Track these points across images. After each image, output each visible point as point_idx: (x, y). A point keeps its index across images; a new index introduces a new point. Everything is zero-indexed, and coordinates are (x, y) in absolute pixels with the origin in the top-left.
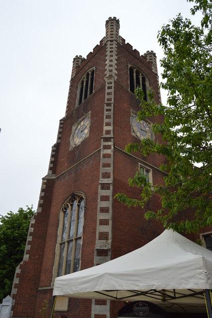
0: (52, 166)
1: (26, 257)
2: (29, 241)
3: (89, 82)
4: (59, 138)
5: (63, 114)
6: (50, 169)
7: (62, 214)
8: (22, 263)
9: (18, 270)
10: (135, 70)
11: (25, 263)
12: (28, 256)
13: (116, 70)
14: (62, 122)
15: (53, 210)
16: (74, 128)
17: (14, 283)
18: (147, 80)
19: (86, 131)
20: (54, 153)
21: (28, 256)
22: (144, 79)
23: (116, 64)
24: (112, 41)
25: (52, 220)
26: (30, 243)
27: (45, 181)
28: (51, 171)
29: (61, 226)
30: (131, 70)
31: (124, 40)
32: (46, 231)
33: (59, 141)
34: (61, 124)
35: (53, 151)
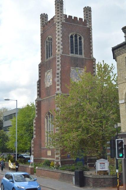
0: (38, 86)
1: (34, 136)
2: (34, 130)
3: (50, 46)
4: (40, 77)
5: (39, 61)
6: (38, 95)
7: (46, 119)
8: (33, 139)
9: (32, 141)
10: (74, 35)
11: (35, 138)
12: (35, 136)
13: (62, 45)
14: (40, 66)
15: (42, 116)
16: (46, 74)
17: (32, 146)
18: (82, 37)
19: (51, 80)
20: (38, 86)
21: (35, 136)
22: (80, 38)
23: (62, 41)
24: (58, 23)
25: (42, 121)
26: (35, 127)
27: (37, 102)
28: (38, 96)
29: (46, 125)
30: (72, 37)
31: (66, 16)
32: (41, 126)
33: (40, 78)
34: (39, 67)
35: (38, 85)
